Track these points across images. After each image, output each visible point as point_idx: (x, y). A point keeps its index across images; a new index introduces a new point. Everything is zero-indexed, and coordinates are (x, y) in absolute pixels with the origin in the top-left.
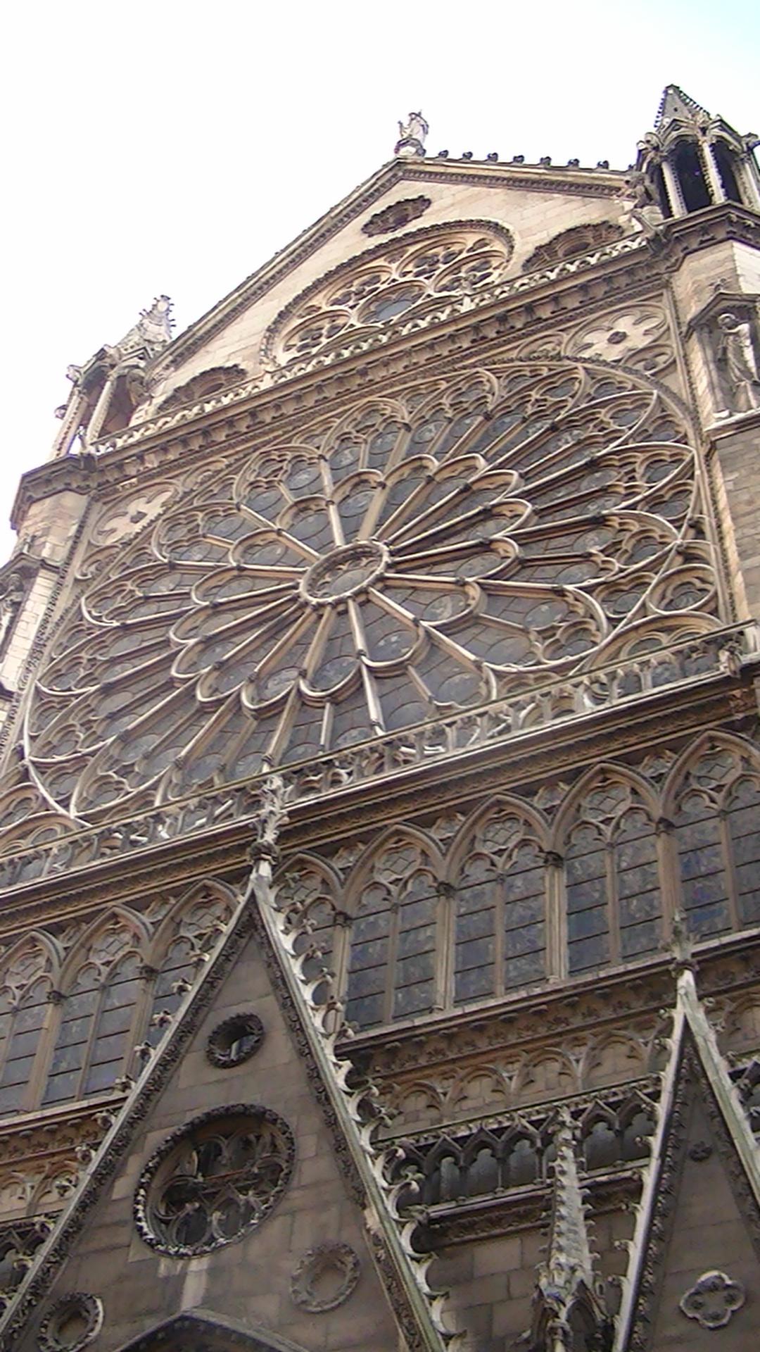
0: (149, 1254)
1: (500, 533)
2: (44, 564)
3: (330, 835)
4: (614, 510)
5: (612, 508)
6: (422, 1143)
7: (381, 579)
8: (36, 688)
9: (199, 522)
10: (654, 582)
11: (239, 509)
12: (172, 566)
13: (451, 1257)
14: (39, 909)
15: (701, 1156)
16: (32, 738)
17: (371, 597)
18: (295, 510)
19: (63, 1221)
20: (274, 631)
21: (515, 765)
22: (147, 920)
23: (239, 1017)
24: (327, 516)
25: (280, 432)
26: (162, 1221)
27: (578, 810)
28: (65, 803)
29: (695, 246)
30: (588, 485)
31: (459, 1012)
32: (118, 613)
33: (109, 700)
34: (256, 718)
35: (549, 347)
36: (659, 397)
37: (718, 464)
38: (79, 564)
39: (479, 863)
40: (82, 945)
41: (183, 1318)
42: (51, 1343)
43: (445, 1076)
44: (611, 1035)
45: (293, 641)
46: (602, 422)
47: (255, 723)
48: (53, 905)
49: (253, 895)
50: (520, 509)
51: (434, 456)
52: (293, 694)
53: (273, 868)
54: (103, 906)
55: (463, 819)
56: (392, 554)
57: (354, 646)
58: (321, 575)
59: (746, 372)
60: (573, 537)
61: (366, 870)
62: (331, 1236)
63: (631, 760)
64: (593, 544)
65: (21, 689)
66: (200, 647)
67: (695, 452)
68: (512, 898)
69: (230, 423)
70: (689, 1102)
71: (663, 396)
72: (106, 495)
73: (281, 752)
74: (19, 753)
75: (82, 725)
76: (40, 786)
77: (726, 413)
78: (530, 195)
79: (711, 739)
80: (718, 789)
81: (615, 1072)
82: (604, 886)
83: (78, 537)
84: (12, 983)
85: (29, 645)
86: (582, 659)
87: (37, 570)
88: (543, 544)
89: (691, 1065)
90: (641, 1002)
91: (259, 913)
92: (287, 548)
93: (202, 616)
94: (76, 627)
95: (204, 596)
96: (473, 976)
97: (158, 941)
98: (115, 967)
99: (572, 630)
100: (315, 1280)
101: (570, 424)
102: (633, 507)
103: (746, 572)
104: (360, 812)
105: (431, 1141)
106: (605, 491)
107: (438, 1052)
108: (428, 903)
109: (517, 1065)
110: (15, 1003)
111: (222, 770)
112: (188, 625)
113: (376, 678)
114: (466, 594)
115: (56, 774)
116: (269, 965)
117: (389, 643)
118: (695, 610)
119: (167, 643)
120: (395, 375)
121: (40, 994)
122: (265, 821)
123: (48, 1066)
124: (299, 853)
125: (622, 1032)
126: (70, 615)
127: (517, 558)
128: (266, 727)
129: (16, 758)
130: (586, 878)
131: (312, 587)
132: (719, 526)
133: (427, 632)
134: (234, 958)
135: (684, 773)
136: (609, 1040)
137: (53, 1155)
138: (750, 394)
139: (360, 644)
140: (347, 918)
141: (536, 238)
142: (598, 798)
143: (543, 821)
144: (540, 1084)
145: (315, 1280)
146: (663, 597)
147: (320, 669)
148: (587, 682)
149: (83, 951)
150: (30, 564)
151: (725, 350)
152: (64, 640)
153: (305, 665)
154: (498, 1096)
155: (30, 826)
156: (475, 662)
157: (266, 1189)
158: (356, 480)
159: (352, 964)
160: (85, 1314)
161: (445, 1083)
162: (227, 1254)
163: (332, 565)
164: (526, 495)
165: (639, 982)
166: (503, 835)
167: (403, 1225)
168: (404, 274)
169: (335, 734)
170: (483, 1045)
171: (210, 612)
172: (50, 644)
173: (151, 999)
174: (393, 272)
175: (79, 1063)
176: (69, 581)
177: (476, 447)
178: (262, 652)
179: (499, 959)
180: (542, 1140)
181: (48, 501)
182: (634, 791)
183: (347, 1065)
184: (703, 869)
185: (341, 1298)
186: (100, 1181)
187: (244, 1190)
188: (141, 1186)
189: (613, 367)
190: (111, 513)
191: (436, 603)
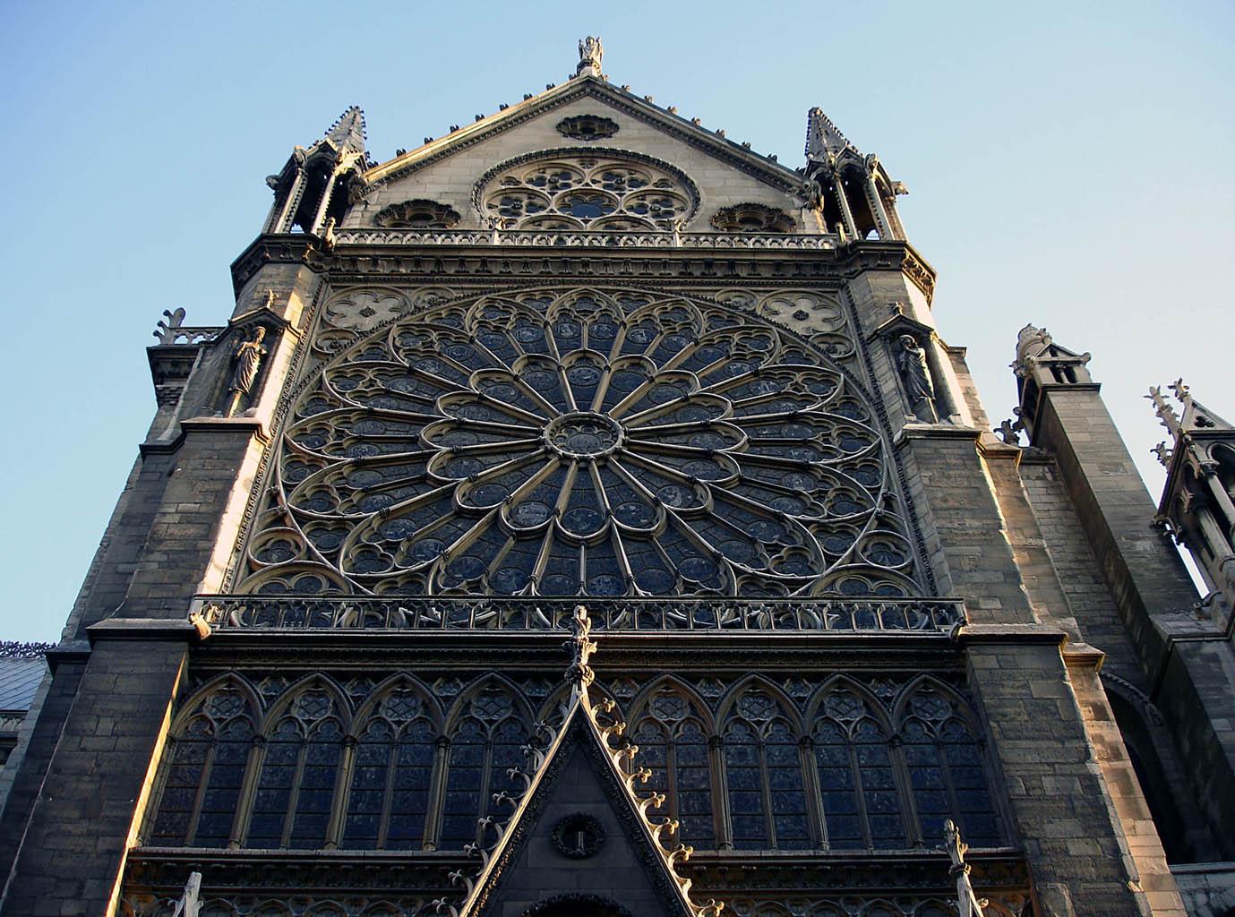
16: (288, 489)
21: (772, 657)
23: (579, 815)
25: (506, 286)
29: (871, 266)
35: (743, 301)
48: (345, 656)
52: (551, 527)
59: (927, 388)
64: (798, 484)
69: (462, 262)
72: (336, 280)
74: (274, 498)
78: (707, 157)
92: (520, 391)
102: (834, 465)
104: (639, 656)
120: (611, 276)
132: (911, 508)
133: (669, 515)
137: (371, 892)
141: (726, 199)
151: (907, 364)
158: (582, 355)
168: (594, 182)
171: (455, 426)
181: (283, 267)
182: (866, 704)
189: (803, 340)
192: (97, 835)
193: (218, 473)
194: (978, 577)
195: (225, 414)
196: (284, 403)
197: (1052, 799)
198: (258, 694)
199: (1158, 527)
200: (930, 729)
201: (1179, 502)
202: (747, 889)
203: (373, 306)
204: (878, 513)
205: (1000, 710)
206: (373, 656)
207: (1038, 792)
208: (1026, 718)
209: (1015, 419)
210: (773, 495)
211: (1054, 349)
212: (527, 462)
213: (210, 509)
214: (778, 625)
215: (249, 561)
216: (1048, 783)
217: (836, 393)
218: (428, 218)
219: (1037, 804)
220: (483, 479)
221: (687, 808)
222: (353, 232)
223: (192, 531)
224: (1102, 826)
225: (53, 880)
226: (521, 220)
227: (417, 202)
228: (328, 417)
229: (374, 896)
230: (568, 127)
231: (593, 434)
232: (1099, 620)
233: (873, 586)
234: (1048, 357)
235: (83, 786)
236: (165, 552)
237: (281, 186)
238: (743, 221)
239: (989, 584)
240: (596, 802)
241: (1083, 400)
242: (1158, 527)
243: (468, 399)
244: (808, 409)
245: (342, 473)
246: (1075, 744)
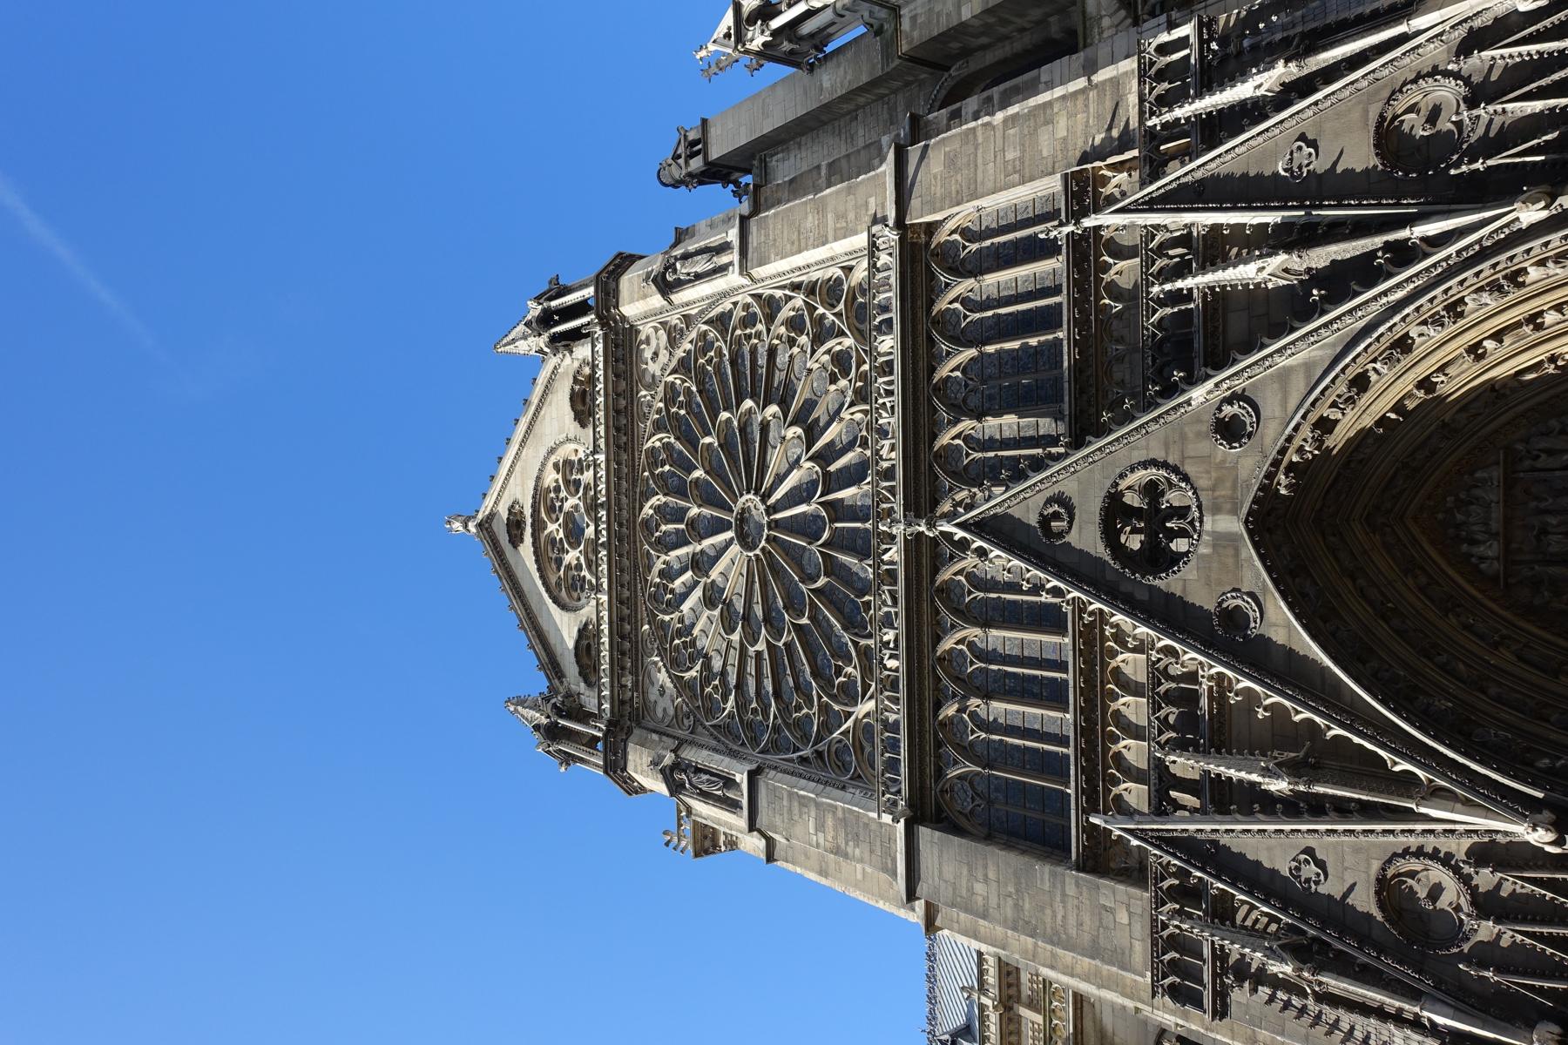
16: (796, 750)
41: (1246, 522)
48: (921, 704)
64: (782, 359)
74: (803, 760)
85: (727, 760)
102: (768, 330)
103: (836, 240)
172: (731, 745)
174: (554, 528)
192: (1064, 895)
194: (851, 216)
196: (733, 754)
197: (1023, 151)
199: (811, 68)
201: (792, 52)
209: (731, 187)
211: (676, 157)
214: (891, 373)
216: (1010, 155)
218: (589, 646)
222: (600, 704)
223: (830, 822)
226: (588, 577)
227: (576, 655)
230: (516, 540)
232: (886, 116)
234: (681, 161)
235: (1027, 906)
237: (568, 759)
238: (584, 403)
239: (856, 207)
241: (714, 132)
242: (811, 68)
244: (725, 352)
246: (979, 132)
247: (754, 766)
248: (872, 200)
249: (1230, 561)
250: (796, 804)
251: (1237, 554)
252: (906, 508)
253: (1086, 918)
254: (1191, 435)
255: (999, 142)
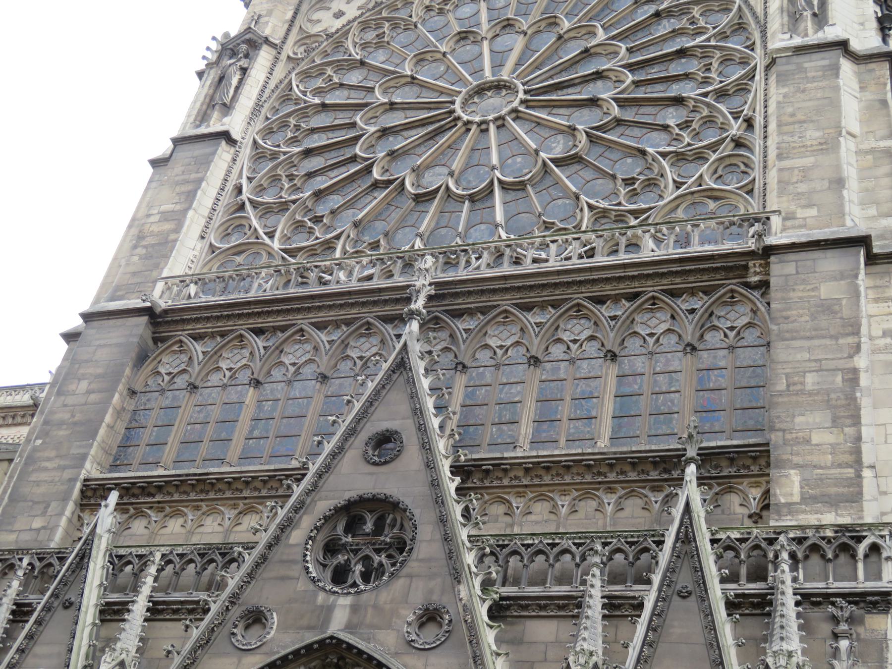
0: (311, 587)
1: (605, 92)
2: (266, 41)
3: (461, 303)
4: (692, 94)
5: (689, 90)
6: (501, 543)
7: (515, 110)
8: (255, 142)
9: (385, 29)
10: (711, 160)
11: (416, 26)
12: (362, 63)
13: (512, 624)
14: (249, 315)
15: (684, 595)
16: (250, 179)
17: (506, 123)
18: (457, 37)
19: (256, 552)
20: (432, 135)
21: (594, 282)
22: (325, 339)
23: (387, 431)
24: (481, 47)
26: (321, 564)
27: (632, 322)
28: (271, 235)
30: (676, 68)
31: (534, 453)
32: (318, 92)
33: (306, 161)
34: (414, 200)
36: (739, 6)
37: (775, 76)
38: (292, 44)
39: (559, 345)
40: (277, 348)
42: (240, 637)
43: (519, 495)
44: (633, 491)
45: (447, 144)
46: (693, 17)
47: (414, 204)
48: (259, 314)
49: (405, 345)
50: (623, 78)
51: (566, 17)
52: (443, 187)
53: (421, 326)
54: (294, 322)
55: (553, 311)
56: (526, 92)
57: (490, 160)
58: (471, 97)
60: (658, 108)
61: (481, 334)
62: (435, 598)
63: (674, 294)
64: (672, 117)
65: (243, 138)
66: (378, 134)
67: (758, 60)
68: (578, 376)
70: (682, 556)
71: (744, 7)
73: (430, 230)
74: (239, 190)
75: (287, 176)
76: (253, 218)
77: (788, 36)
79: (732, 291)
80: (732, 328)
81: (633, 517)
82: (642, 381)
83: (292, 22)
84: (224, 365)
86: (650, 209)
87: (261, 44)
88: (635, 109)
89: (687, 531)
90: (657, 473)
91: (408, 358)
93: (381, 109)
94: (286, 97)
95: (385, 92)
96: (545, 426)
97: (331, 356)
98: (299, 368)
99: (647, 183)
100: (422, 626)
101: (668, 13)
102: (705, 95)
103: (781, 170)
105: (506, 542)
106: (687, 76)
107: (516, 478)
108: (521, 367)
109: (567, 498)
110: (225, 381)
111: (386, 235)
112: (370, 115)
113: (503, 188)
114: (574, 136)
115: (265, 210)
116: (412, 398)
117: (515, 163)
118: (737, 188)
119: (353, 125)
121: (244, 377)
122: (419, 291)
123: (245, 432)
124: (437, 312)
125: (643, 491)
126: (283, 86)
127: (615, 117)
128: (421, 208)
129: (236, 191)
130: (630, 373)
131: (465, 103)
132: (766, 127)
133: (544, 164)
134: (388, 387)
135: (709, 312)
136: (631, 494)
137: (246, 498)
138: (809, 24)
139: (495, 160)
140: (464, 367)
142: (648, 315)
143: (607, 326)
144: (581, 514)
145: (422, 626)
146: (715, 172)
147: (462, 172)
148: (653, 231)
149: (278, 352)
150: (255, 38)
152: (276, 104)
153: (453, 168)
154: (553, 517)
155: (243, 248)
156: (574, 193)
157: (393, 553)
159: (464, 400)
160: (264, 621)
161: (519, 500)
162: (364, 596)
163: (480, 91)
164: (631, 67)
165: (658, 459)
166: (578, 328)
167: (484, 601)
169: (469, 226)
170: (547, 479)
172: (266, 106)
173: (322, 396)
175: (267, 431)
176: (283, 56)
177: (597, 15)
178: (423, 148)
179: (565, 419)
180: (581, 558)
182: (673, 317)
183: (458, 480)
184: (711, 385)
185: (438, 643)
186: (282, 530)
187: (378, 551)
188: (310, 538)
190: (318, 6)
191: (552, 139)
193: (194, 176)
194: (802, 188)
195: (208, 126)
197: (810, 394)
198: (458, 329)
200: (726, 336)
202: (525, 483)
203: (344, 7)
204: (734, 136)
205: (784, 314)
206: (279, 312)
207: (799, 387)
208: (807, 318)
210: (645, 131)
212: (439, 131)
213: (178, 207)
215: (211, 244)
216: (811, 380)
217: (724, 20)
219: (794, 398)
220: (400, 151)
221: (500, 417)
223: (167, 226)
224: (852, 416)
225: (30, 503)
228: (289, 115)
229: (247, 501)
231: (502, 97)
233: (712, 205)
235: (61, 433)
236: (145, 247)
240: (403, 419)
243: (403, 81)
245: (292, 162)
246: (851, 340)
247: (235, 135)
248: (813, 212)
249: (305, 622)
250: (190, 187)
251: (310, 628)
252: (438, 285)
253: (42, 489)
254: (432, 584)
255: (832, 365)
